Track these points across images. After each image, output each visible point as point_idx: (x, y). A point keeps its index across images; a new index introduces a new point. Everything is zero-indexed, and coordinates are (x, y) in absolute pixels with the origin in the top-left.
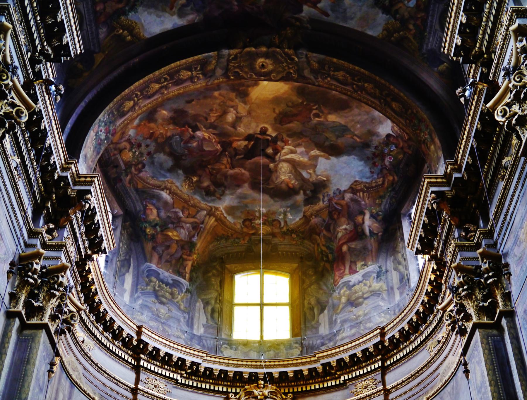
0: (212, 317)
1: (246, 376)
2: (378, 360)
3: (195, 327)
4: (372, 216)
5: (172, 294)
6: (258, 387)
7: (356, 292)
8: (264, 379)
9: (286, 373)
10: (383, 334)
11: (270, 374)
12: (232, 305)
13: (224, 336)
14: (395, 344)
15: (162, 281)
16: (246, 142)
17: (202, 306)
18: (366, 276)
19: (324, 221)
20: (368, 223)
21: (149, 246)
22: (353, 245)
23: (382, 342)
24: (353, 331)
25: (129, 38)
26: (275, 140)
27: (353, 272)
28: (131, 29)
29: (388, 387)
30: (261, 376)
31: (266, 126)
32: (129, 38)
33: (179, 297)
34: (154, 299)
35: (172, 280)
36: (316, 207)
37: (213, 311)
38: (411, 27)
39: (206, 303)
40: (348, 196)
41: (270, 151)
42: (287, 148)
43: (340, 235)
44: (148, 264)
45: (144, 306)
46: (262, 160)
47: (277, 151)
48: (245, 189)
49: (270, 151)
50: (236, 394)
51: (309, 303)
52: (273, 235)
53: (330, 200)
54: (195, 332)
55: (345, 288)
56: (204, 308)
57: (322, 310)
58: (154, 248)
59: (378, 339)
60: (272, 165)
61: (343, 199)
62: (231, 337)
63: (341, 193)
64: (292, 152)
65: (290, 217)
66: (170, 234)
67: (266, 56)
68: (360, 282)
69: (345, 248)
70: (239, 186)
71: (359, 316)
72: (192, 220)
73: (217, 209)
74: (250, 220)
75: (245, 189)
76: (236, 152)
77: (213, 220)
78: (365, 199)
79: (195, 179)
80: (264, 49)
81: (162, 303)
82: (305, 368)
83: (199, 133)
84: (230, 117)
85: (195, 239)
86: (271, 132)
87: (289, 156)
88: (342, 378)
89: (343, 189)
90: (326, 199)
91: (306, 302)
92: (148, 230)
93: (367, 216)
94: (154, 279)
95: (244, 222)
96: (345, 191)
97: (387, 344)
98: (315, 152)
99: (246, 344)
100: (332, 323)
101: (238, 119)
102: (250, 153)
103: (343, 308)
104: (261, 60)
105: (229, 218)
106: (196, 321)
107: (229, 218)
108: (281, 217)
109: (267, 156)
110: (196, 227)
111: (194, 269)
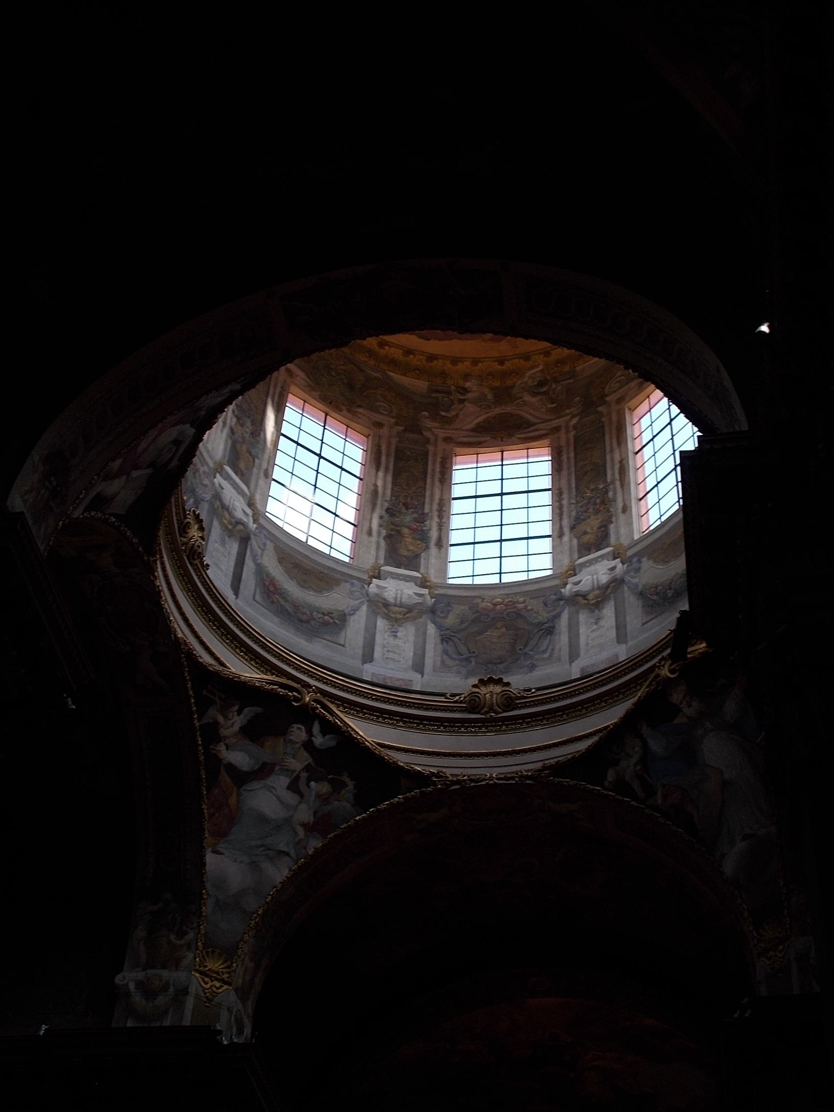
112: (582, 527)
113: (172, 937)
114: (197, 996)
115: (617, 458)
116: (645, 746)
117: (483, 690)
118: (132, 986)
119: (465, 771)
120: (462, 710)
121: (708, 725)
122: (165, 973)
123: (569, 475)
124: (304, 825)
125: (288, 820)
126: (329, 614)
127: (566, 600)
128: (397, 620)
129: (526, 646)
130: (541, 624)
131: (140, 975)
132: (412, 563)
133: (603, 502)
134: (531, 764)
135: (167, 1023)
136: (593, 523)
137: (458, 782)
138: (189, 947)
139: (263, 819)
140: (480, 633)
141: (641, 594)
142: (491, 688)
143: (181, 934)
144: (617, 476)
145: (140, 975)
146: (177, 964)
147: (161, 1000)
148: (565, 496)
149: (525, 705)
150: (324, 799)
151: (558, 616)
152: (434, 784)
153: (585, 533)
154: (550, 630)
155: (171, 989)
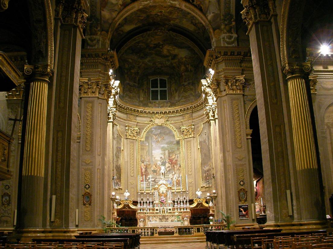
0: (145, 94)
3: (141, 98)
4: (191, 66)
5: (134, 89)
7: (186, 88)
15: (131, 86)
16: (154, 45)
17: (142, 91)
18: (189, 84)
19: (177, 65)
21: (126, 76)
22: (186, 73)
24: (185, 100)
25: (122, 33)
26: (162, 45)
27: (185, 82)
28: (122, 31)
31: (160, 42)
32: (122, 33)
33: (136, 90)
34: (129, 92)
35: (133, 85)
37: (145, 92)
38: (201, 30)
39: (143, 90)
40: (184, 59)
41: (161, 47)
43: (182, 70)
44: (126, 81)
45: (127, 95)
46: (159, 49)
47: (163, 47)
49: (161, 47)
51: (173, 89)
52: (162, 67)
53: (179, 60)
54: (141, 100)
55: (183, 86)
56: (143, 92)
57: (176, 92)
58: (128, 76)
60: (161, 50)
61: (183, 60)
66: (132, 71)
67: (160, 32)
68: (187, 85)
69: (183, 74)
71: (187, 95)
72: (138, 66)
79: (138, 55)
80: (159, 31)
81: (131, 92)
83: (140, 44)
84: (149, 40)
85: (139, 71)
86: (161, 43)
89: (183, 57)
91: (172, 89)
92: (125, 71)
93: (190, 66)
94: (128, 86)
95: (153, 64)
100: (179, 96)
102: (155, 48)
103: (182, 92)
105: (149, 63)
106: (140, 96)
107: (149, 63)
109: (160, 48)
110: (139, 67)
111: (139, 80)
113: (95, 29)
114: (102, 41)
118: (88, 39)
122: (95, 37)
124: (120, 5)
125: (117, 3)
131: (89, 37)
135: (96, 47)
138: (99, 31)
139: (112, 4)
143: (97, 28)
145: (89, 37)
146: (97, 34)
147: (94, 42)
155: (96, 40)
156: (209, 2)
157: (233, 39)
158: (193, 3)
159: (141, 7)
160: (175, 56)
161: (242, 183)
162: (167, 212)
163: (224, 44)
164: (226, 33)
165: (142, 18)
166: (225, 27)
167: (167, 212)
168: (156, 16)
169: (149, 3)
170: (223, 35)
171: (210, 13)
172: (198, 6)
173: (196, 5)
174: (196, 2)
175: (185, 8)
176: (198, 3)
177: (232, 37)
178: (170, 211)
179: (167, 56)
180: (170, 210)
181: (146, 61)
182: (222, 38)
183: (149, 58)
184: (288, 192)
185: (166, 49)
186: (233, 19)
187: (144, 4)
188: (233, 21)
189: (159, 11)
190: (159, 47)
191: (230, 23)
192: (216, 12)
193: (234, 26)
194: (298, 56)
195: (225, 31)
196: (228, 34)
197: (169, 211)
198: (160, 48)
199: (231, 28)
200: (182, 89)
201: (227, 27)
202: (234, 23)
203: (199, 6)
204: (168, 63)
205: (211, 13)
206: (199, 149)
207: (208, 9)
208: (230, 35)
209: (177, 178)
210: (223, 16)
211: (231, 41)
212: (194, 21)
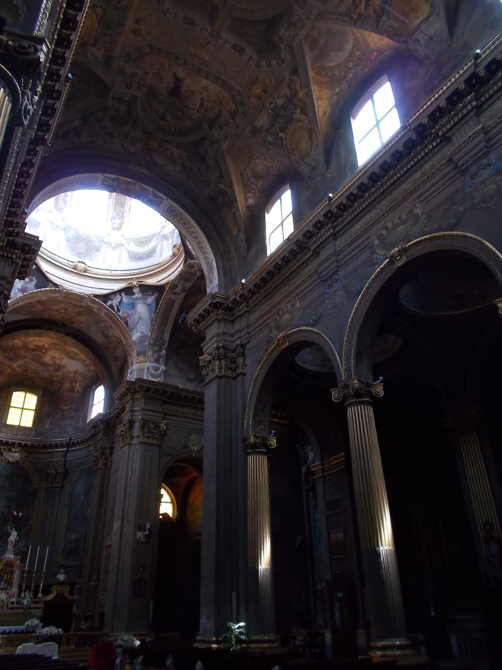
1: (10, 443)
2: (65, 448)
4: (80, 385)
6: (14, 448)
8: (18, 445)
9: (27, 444)
10: (70, 440)
11: (21, 443)
12: (9, 406)
13: (3, 422)
14: (74, 445)
20: (78, 387)
23: (69, 443)
26: (47, 349)
27: (66, 405)
29: (67, 459)
30: (17, 444)
36: (57, 374)
41: (44, 351)
42: (52, 352)
43: (64, 388)
46: (40, 353)
47: (46, 352)
48: (28, 360)
50: (4, 449)
53: (64, 373)
59: (68, 441)
60: (43, 355)
61: (70, 374)
62: (6, 422)
63: (70, 373)
64: (53, 353)
65: (44, 373)
68: (67, 410)
69: (65, 394)
70: (26, 358)
73: (13, 365)
74: (27, 371)
75: (28, 360)
76: (29, 349)
77: (9, 370)
78: (79, 378)
79: (6, 354)
82: (36, 444)
86: (47, 346)
87: (51, 354)
88: (50, 450)
90: (63, 372)
95: (24, 370)
96: (71, 372)
97: (71, 443)
98: (64, 356)
99: (12, 426)
101: (34, 340)
104: (51, 334)
105: (17, 369)
108: (41, 372)
109: (43, 352)
112: (114, 221)
115: (129, 204)
116: (122, 299)
117: (79, 264)
119: (69, 287)
120: (71, 268)
121: (141, 301)
123: (113, 201)
126: (36, 221)
127: (105, 243)
128: (54, 229)
129: (91, 252)
130: (96, 247)
132: (61, 210)
133: (122, 216)
134: (88, 291)
136: (118, 221)
137: (66, 289)
140: (78, 242)
141: (128, 252)
142: (81, 264)
144: (128, 210)
148: (111, 207)
149: (90, 273)
150: (27, 283)
151: (101, 246)
152: (59, 288)
153: (115, 223)
154: (98, 250)
156: (140, 317)
157: (159, 372)
158: (118, 313)
159: (44, 298)
160: (59, 368)
161: (141, 569)
162: (7, 606)
163: (147, 376)
164: (153, 362)
165: (36, 310)
166: (153, 354)
167: (7, 606)
168: (57, 312)
169: (57, 297)
170: (148, 364)
171: (137, 332)
172: (123, 318)
173: (121, 316)
174: (122, 313)
175: (104, 316)
176: (125, 315)
177: (159, 368)
178: (11, 606)
179: (49, 365)
180: (12, 603)
181: (15, 365)
182: (146, 367)
183: (20, 362)
184: (234, 595)
185: (50, 355)
186: (164, 347)
187: (50, 296)
188: (165, 349)
189: (64, 307)
190: (41, 351)
191: (160, 351)
192: (146, 333)
193: (164, 355)
194: (263, 428)
195: (152, 359)
196: (154, 364)
197: (10, 606)
198: (43, 352)
199: (160, 357)
200: (59, 416)
201: (155, 356)
202: (164, 352)
203: (124, 319)
204: (46, 374)
205: (139, 332)
206: (66, 505)
207: (135, 326)
208: (157, 365)
209: (21, 548)
210: (153, 339)
211: (157, 373)
212: (106, 332)
